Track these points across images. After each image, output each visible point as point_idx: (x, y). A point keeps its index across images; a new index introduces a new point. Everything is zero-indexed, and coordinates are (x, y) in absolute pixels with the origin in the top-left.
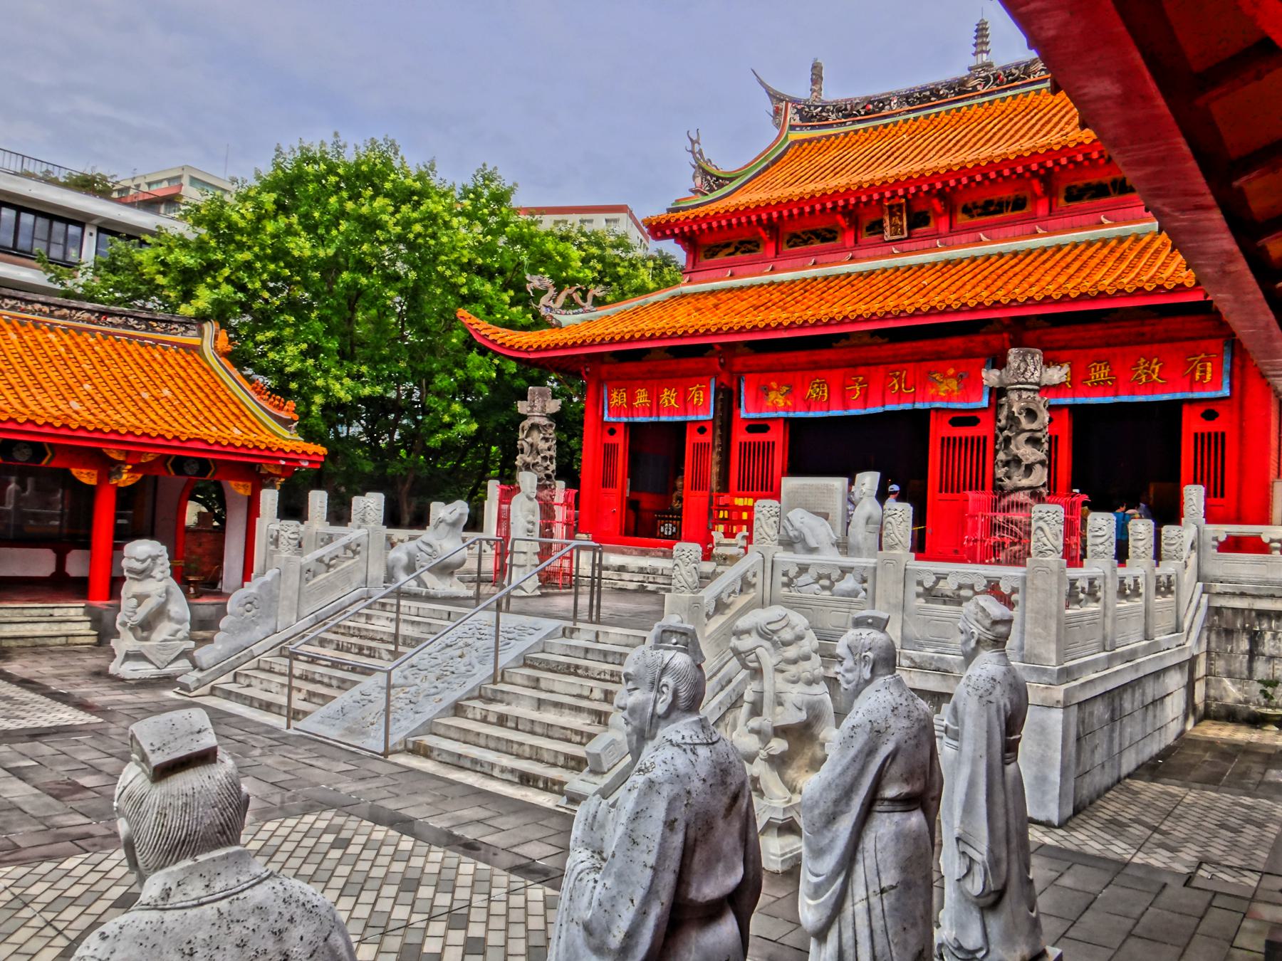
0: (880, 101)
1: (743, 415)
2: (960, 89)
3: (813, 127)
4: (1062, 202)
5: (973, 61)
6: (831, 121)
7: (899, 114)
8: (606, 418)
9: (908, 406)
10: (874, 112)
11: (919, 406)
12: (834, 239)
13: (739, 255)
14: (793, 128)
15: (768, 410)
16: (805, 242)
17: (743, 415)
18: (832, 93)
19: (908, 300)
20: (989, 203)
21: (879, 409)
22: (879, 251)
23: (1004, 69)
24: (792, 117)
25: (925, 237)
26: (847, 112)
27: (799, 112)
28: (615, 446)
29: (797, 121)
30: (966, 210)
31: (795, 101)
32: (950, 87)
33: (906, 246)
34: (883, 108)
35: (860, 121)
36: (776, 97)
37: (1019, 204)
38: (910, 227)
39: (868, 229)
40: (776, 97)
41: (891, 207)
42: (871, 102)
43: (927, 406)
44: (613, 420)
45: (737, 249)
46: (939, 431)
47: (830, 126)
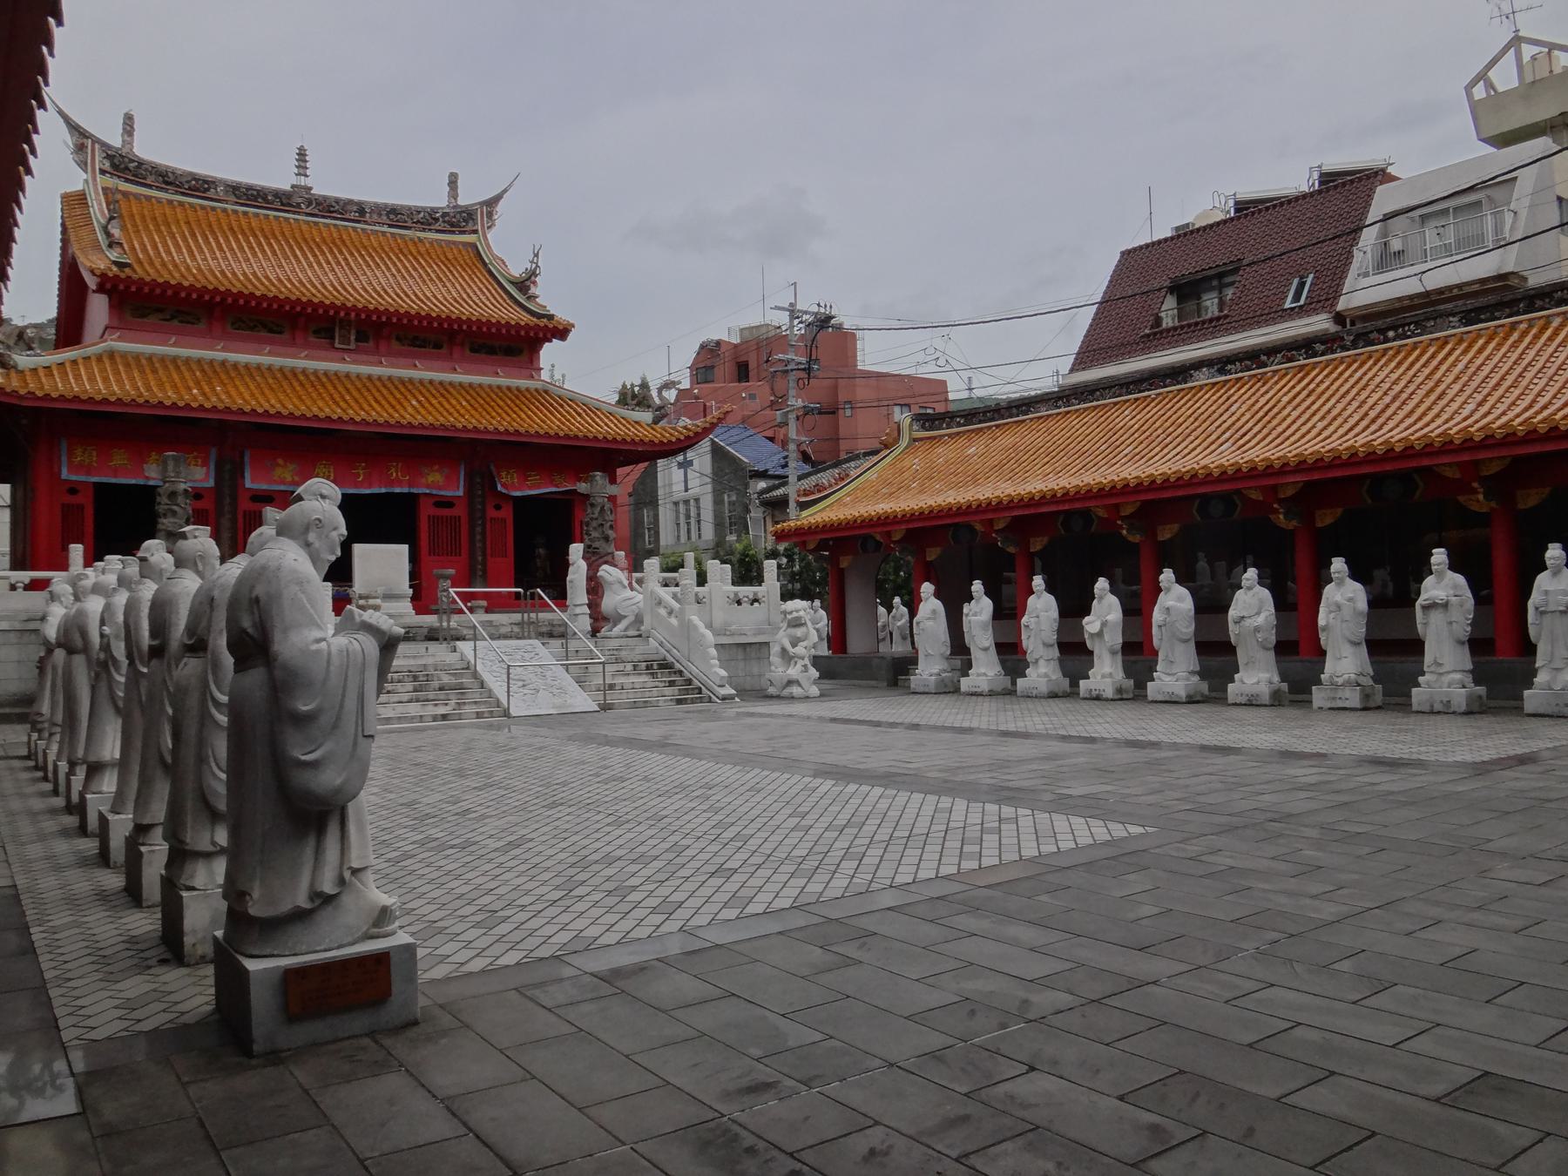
0: (205, 182)
1: (248, 484)
2: (283, 200)
3: (127, 180)
4: (468, 352)
5: (294, 180)
6: (148, 182)
7: (227, 202)
8: (65, 474)
9: (406, 490)
10: (197, 190)
11: (415, 491)
12: (281, 333)
13: (175, 322)
14: (103, 172)
15: (275, 482)
16: (252, 329)
17: (248, 484)
18: (146, 149)
19: (413, 414)
20: (416, 338)
21: (383, 490)
22: (333, 354)
23: (325, 198)
24: (99, 161)
25: (366, 352)
26: (167, 179)
27: (108, 157)
28: (81, 508)
29: (107, 165)
30: (398, 339)
31: (103, 144)
32: (278, 194)
33: (354, 356)
34: (207, 190)
35: (183, 194)
36: (74, 128)
37: (438, 346)
38: (357, 340)
39: (315, 332)
40: (74, 128)
41: (341, 321)
42: (197, 180)
43: (420, 491)
44: (74, 478)
45: (173, 318)
46: (426, 511)
47: (150, 186)
